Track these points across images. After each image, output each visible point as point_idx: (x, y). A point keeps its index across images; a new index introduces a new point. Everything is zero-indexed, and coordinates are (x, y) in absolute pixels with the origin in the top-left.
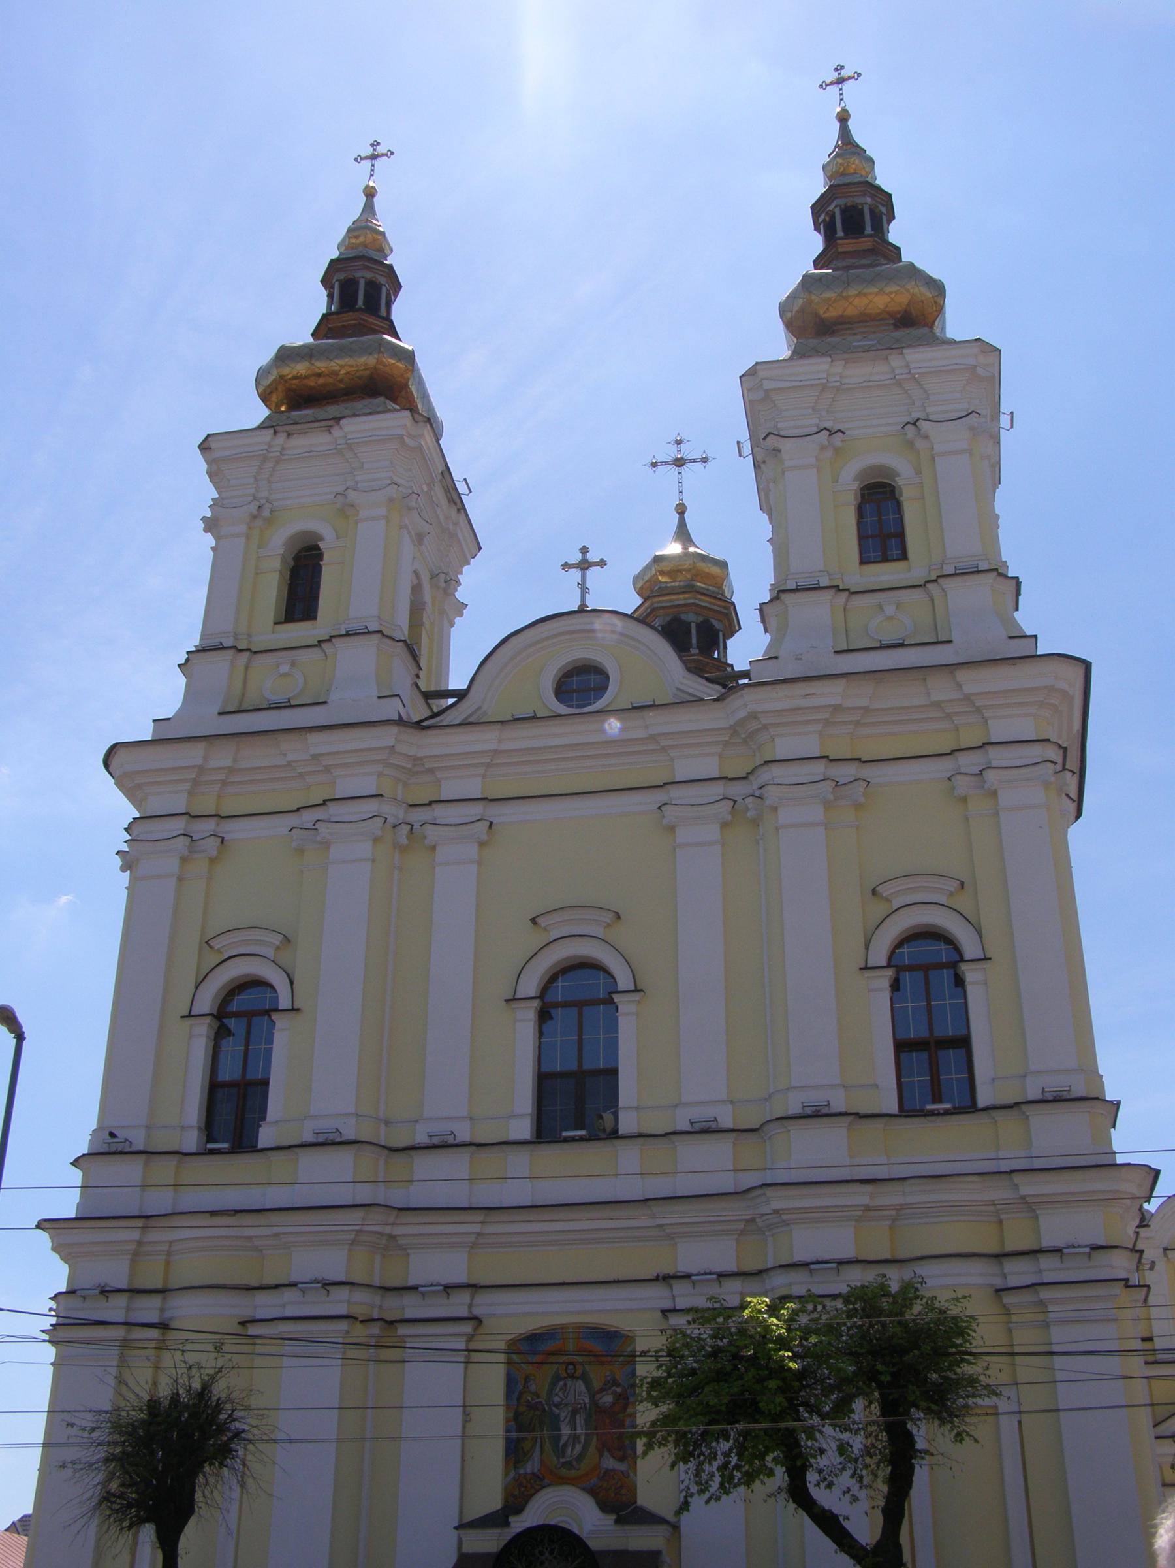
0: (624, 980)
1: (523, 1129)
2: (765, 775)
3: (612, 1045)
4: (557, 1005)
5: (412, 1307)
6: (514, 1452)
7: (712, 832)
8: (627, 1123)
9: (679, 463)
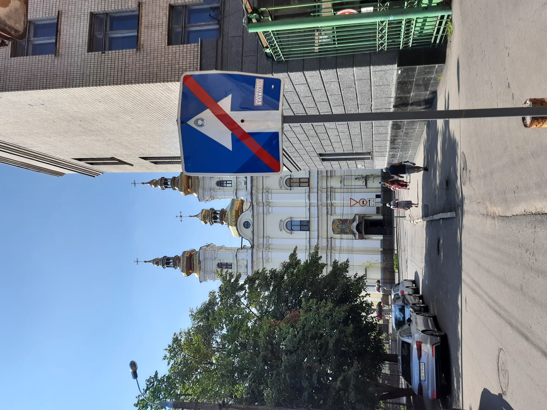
0: (290, 219)
1: (308, 232)
2: (264, 201)
3: (297, 221)
4: (291, 228)
5: (329, 245)
6: (347, 233)
7: (270, 208)
8: (308, 219)
9: (181, 216)
